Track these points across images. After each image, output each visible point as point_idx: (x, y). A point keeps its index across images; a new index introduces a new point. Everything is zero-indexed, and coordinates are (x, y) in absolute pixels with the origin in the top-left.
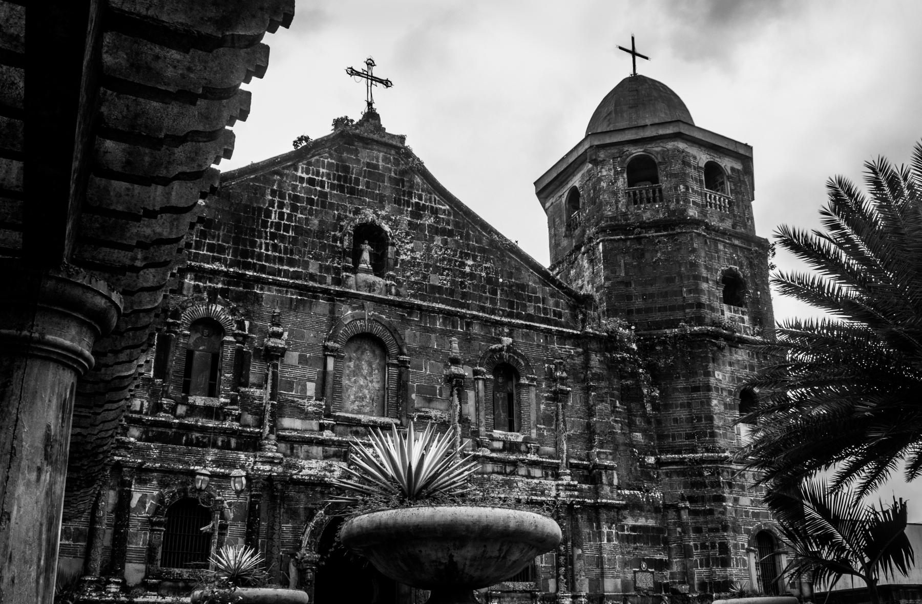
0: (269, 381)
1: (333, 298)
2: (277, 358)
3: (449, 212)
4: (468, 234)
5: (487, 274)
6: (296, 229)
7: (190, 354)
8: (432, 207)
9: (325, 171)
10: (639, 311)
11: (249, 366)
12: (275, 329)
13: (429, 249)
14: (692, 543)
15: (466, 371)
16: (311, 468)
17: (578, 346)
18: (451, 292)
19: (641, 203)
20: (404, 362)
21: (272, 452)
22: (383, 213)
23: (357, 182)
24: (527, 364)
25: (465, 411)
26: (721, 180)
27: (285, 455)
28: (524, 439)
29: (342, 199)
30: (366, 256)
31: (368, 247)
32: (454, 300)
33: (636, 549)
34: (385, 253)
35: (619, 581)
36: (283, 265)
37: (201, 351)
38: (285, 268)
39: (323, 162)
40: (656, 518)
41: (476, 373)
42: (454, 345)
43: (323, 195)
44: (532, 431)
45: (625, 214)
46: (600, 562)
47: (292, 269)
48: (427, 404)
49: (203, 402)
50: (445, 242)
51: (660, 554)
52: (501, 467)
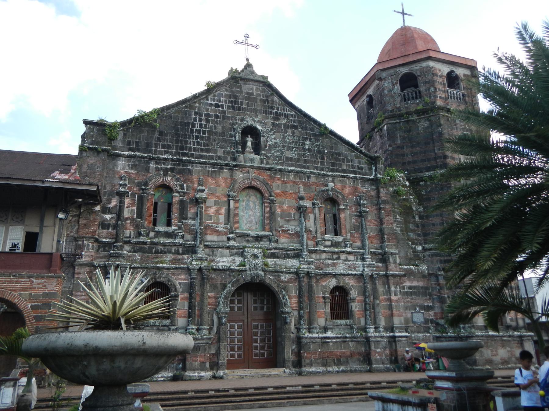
0: (199, 216)
3: (295, 115)
4: (306, 127)
5: (318, 148)
6: (209, 132)
7: (156, 204)
8: (285, 114)
9: (223, 99)
10: (409, 163)
11: (187, 208)
12: (201, 187)
13: (284, 137)
14: (446, 296)
15: (308, 204)
16: (223, 262)
17: (373, 185)
18: (298, 160)
19: (409, 100)
21: (201, 254)
22: (257, 119)
23: (242, 103)
24: (343, 198)
26: (457, 83)
27: (209, 255)
29: (234, 114)
30: (249, 144)
32: (300, 165)
33: (412, 299)
34: (260, 142)
35: (402, 318)
37: (161, 202)
38: (205, 154)
39: (222, 94)
40: (424, 281)
41: (314, 204)
43: (224, 112)
44: (348, 234)
45: (399, 107)
46: (390, 307)
47: (208, 155)
50: (293, 133)
51: (427, 302)
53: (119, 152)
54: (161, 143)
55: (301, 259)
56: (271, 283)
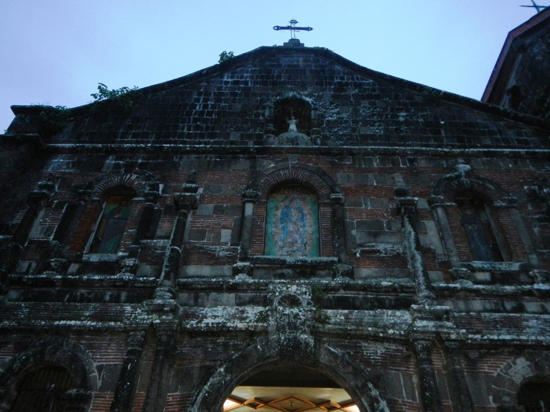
1: (251, 156)
2: (186, 207)
5: (424, 119)
6: (218, 113)
12: (188, 185)
13: (356, 111)
16: (215, 317)
20: (337, 200)
22: (306, 93)
23: (279, 76)
25: (425, 240)
28: (521, 266)
31: (294, 121)
36: (204, 139)
41: (430, 202)
42: (397, 179)
47: (212, 141)
48: (372, 239)
49: (98, 258)
52: (496, 304)
53: (57, 145)
54: (133, 131)
55: (414, 306)
56: (333, 365)
